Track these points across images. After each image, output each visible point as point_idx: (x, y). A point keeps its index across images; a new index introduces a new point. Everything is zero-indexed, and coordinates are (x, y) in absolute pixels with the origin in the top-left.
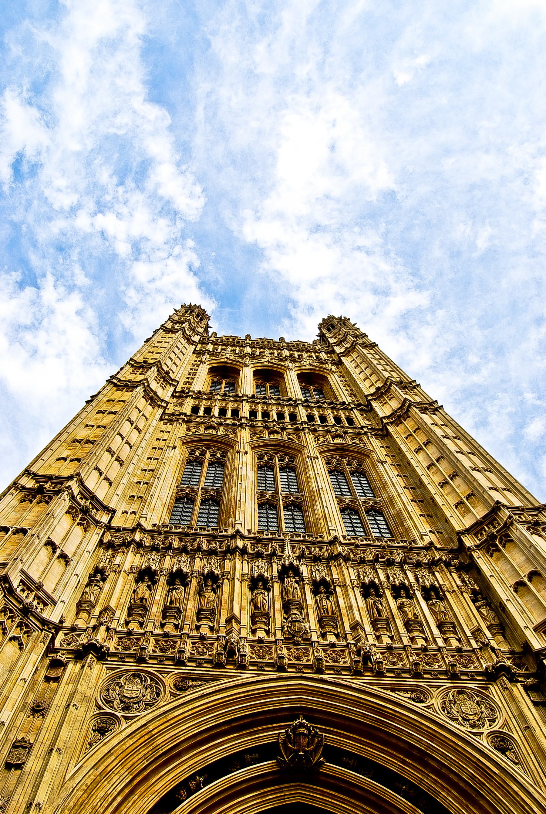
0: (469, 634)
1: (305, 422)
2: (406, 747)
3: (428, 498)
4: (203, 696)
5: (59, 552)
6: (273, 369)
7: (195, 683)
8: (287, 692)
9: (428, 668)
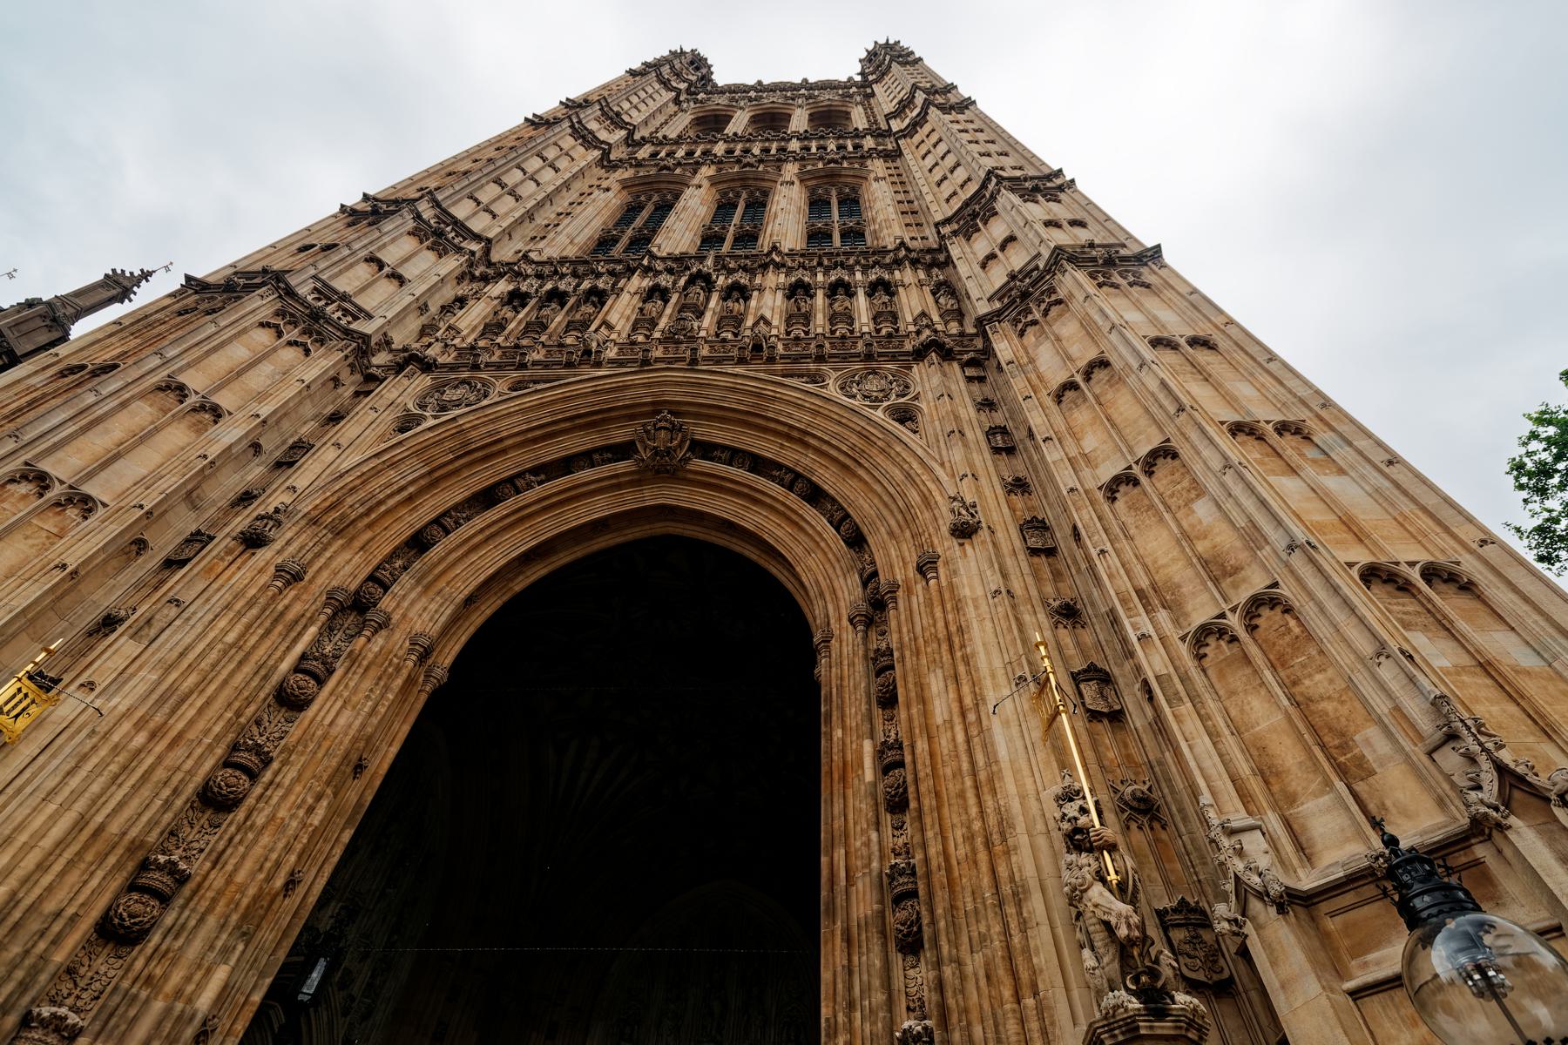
2: (785, 429)
4: (536, 391)
5: (386, 270)
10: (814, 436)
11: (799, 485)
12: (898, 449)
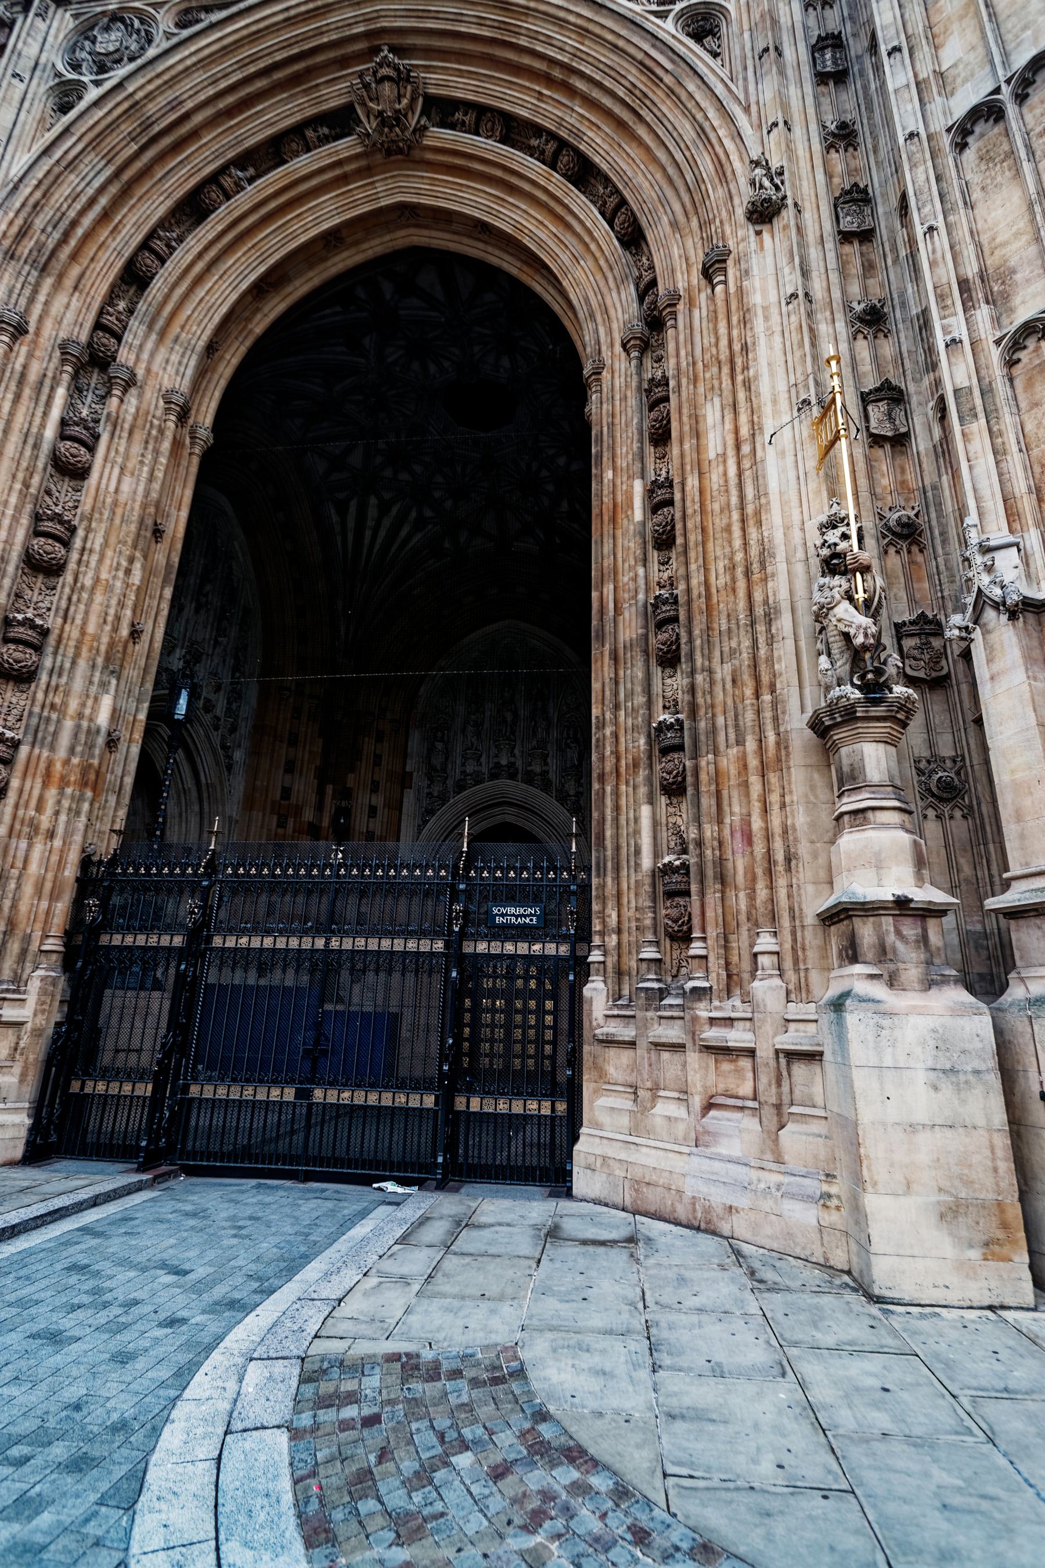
4: (213, 26)
10: (582, 75)
12: (691, 87)
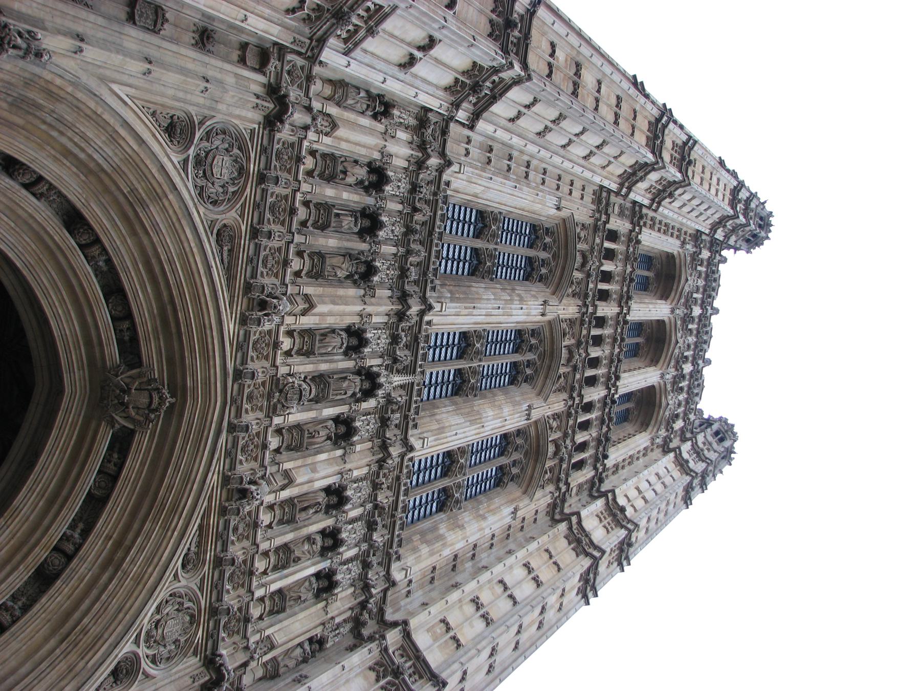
0: (268, 632)
1: (581, 400)
3: (459, 579)
6: (665, 350)
7: (225, 254)
8: (207, 382)
9: (227, 575)
10: (111, 579)
11: (58, 560)
